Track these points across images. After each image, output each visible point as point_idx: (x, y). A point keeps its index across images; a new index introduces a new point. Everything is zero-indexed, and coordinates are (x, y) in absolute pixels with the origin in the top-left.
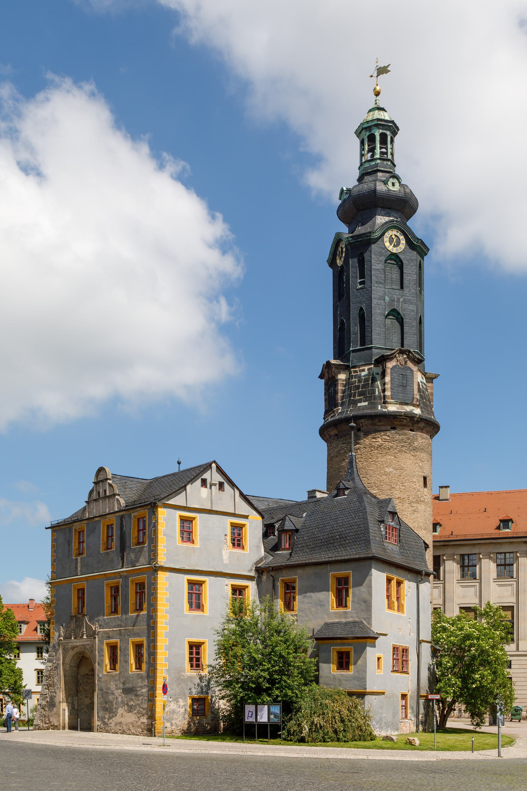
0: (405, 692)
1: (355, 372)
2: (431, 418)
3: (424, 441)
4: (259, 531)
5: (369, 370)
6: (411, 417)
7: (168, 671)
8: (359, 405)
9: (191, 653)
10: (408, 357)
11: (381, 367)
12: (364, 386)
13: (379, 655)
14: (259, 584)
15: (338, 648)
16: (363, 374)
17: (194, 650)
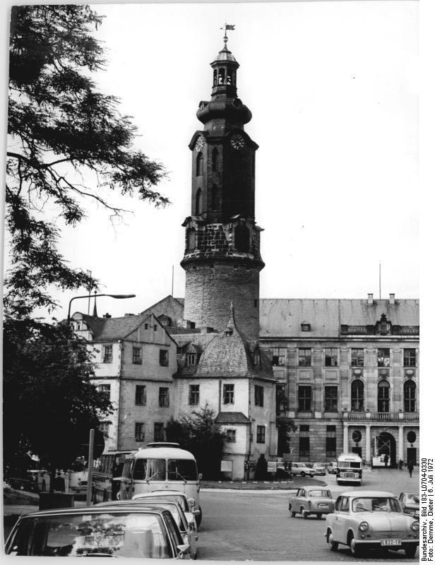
1: (210, 227)
8: (213, 250)
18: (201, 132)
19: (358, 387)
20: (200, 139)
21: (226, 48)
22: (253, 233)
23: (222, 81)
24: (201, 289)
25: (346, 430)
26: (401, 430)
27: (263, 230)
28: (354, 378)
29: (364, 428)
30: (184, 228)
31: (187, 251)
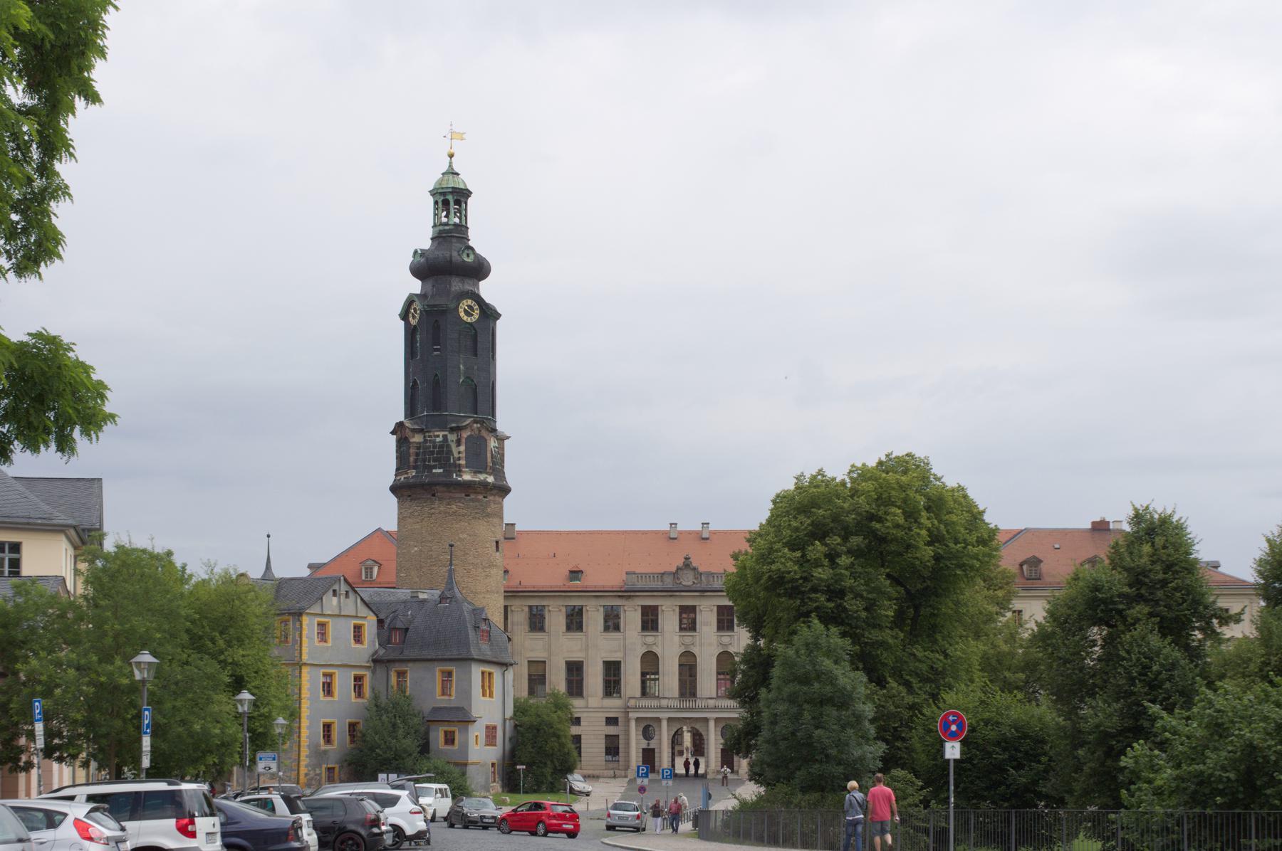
0: (495, 761)
1: (429, 436)
2: (504, 485)
3: (496, 506)
4: (374, 629)
5: (443, 436)
6: (484, 485)
7: (309, 746)
8: (434, 471)
9: (324, 731)
10: (482, 425)
11: (455, 435)
12: (438, 453)
13: (476, 734)
14: (374, 672)
15: (446, 728)
16: (438, 440)
17: (326, 729)
18: (417, 295)
19: (650, 662)
20: (414, 305)
21: (450, 166)
22: (493, 443)
23: (446, 216)
24: (417, 526)
25: (633, 724)
26: (712, 724)
27: (508, 438)
28: (644, 650)
29: (658, 720)
30: (395, 436)
31: (399, 470)
